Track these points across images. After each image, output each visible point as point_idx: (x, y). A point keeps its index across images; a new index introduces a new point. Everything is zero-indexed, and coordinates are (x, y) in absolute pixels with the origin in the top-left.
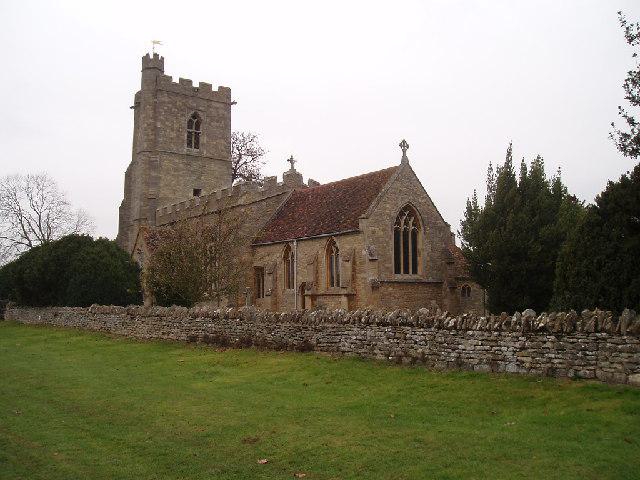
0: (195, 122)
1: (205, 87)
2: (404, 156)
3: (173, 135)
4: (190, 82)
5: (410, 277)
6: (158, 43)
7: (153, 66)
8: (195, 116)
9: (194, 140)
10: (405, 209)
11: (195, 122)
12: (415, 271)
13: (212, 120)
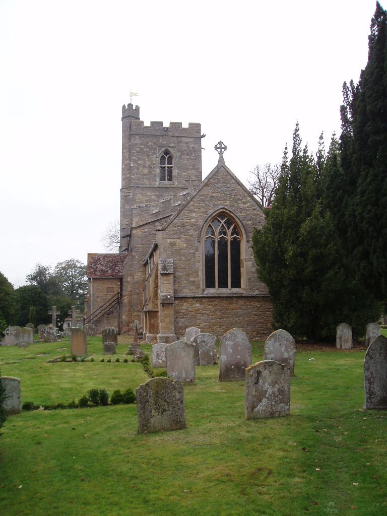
0: (167, 157)
1: (176, 126)
2: (221, 160)
3: (146, 171)
4: (161, 123)
5: (228, 291)
6: (136, 95)
7: (130, 115)
8: (167, 152)
9: (167, 174)
10: (222, 215)
11: (167, 157)
12: (236, 283)
13: (182, 154)
